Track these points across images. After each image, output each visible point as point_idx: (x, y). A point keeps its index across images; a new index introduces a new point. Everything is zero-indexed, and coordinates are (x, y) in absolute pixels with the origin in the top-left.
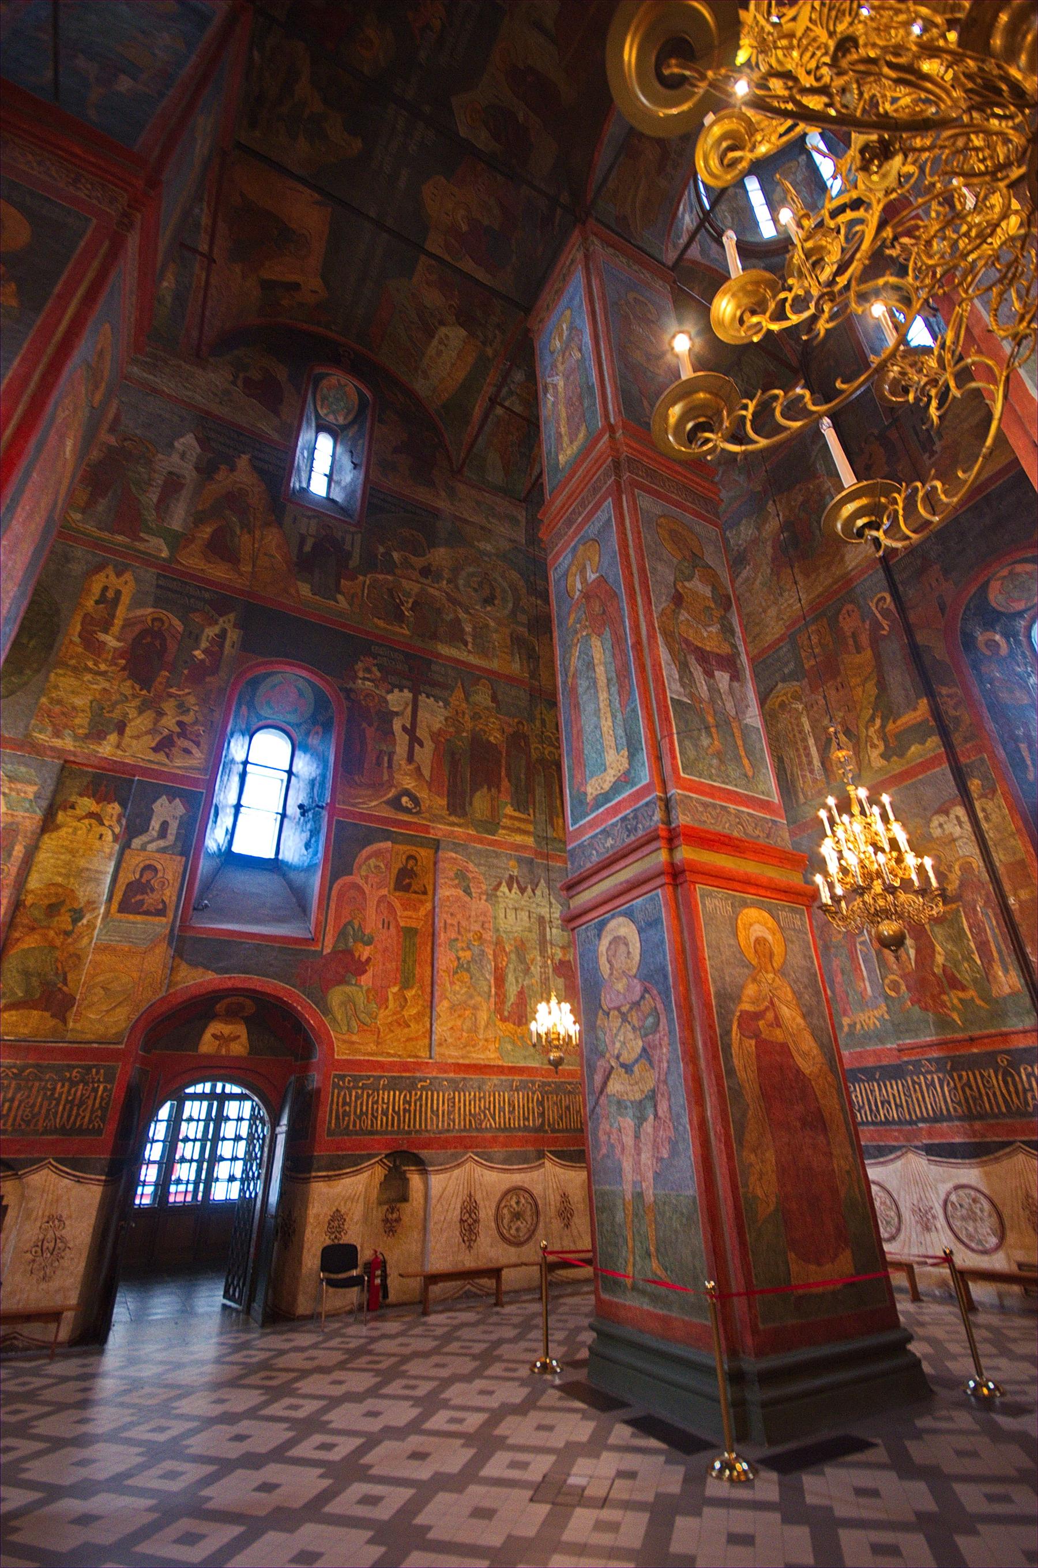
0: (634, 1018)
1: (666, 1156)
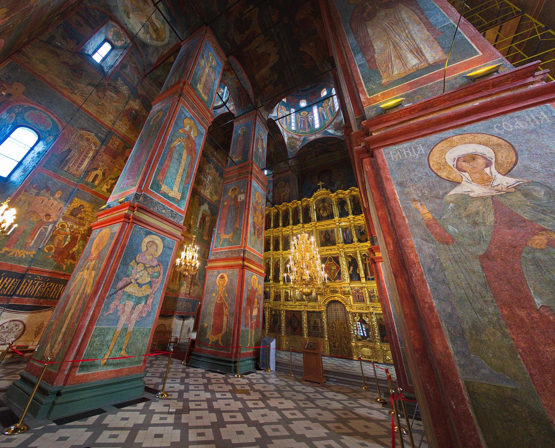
0: (150, 270)
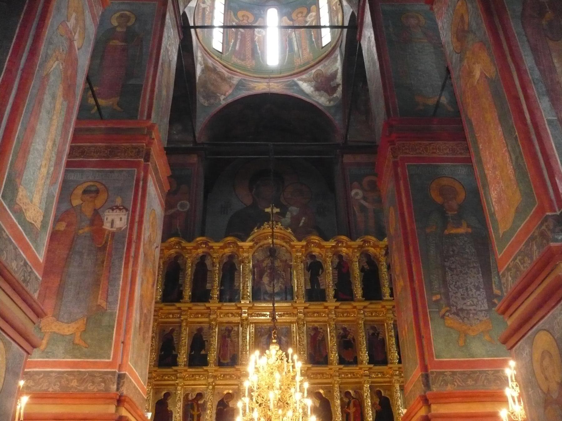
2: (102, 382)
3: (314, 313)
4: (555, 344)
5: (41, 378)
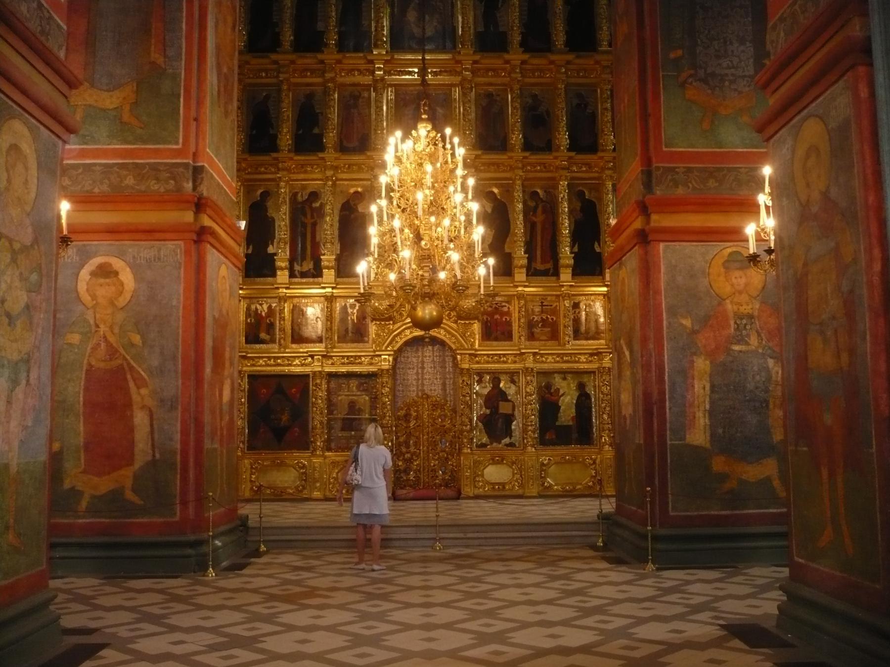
1: (30, 424)
2: (170, 178)
3: (488, 70)
4: (827, 137)
5: (80, 174)
